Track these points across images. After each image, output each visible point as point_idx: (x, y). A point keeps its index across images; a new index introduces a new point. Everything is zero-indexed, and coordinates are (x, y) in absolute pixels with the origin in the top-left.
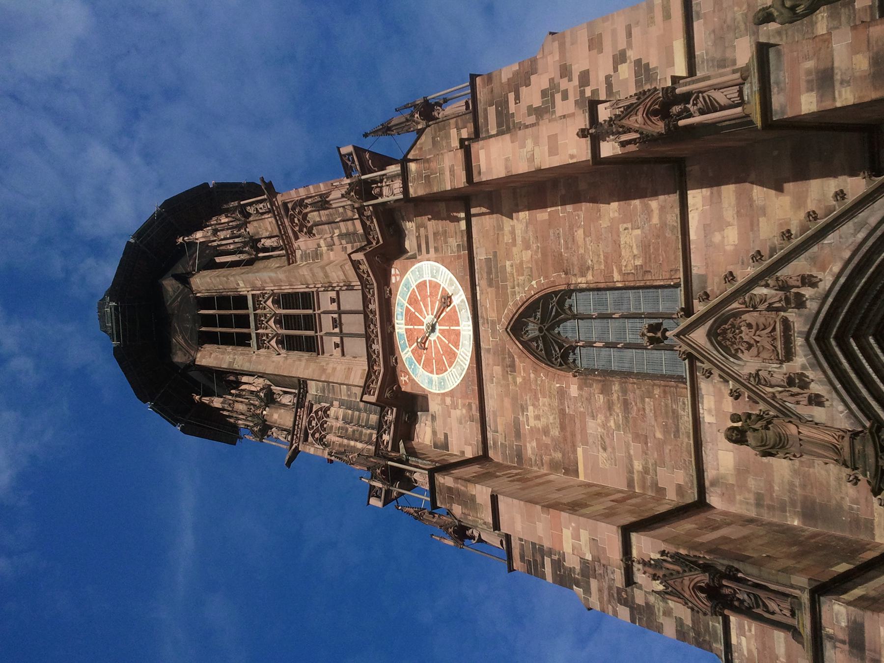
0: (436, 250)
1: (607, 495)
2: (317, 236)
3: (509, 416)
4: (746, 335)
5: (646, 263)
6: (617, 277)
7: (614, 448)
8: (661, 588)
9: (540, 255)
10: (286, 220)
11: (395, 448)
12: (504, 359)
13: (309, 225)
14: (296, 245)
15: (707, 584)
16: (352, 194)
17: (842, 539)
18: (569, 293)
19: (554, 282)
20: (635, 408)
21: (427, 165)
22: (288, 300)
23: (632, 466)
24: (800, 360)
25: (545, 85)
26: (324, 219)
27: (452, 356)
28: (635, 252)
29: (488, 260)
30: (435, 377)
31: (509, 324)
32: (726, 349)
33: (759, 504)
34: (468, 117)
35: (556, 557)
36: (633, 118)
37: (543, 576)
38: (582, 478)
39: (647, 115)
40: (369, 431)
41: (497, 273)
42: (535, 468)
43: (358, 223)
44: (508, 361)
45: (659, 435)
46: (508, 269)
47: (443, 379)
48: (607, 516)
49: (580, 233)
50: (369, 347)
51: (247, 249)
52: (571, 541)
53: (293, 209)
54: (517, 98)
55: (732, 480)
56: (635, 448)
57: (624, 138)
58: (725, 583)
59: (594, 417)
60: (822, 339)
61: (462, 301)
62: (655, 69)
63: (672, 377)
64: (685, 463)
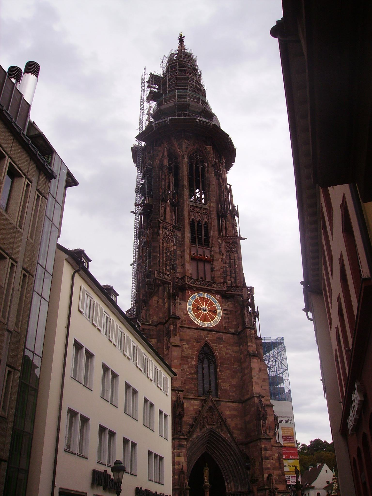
0: (225, 317)
6: (220, 381)
24: (208, 427)
29: (222, 339)
30: (191, 308)
44: (199, 340)
47: (191, 311)
49: (229, 372)
60: (211, 431)
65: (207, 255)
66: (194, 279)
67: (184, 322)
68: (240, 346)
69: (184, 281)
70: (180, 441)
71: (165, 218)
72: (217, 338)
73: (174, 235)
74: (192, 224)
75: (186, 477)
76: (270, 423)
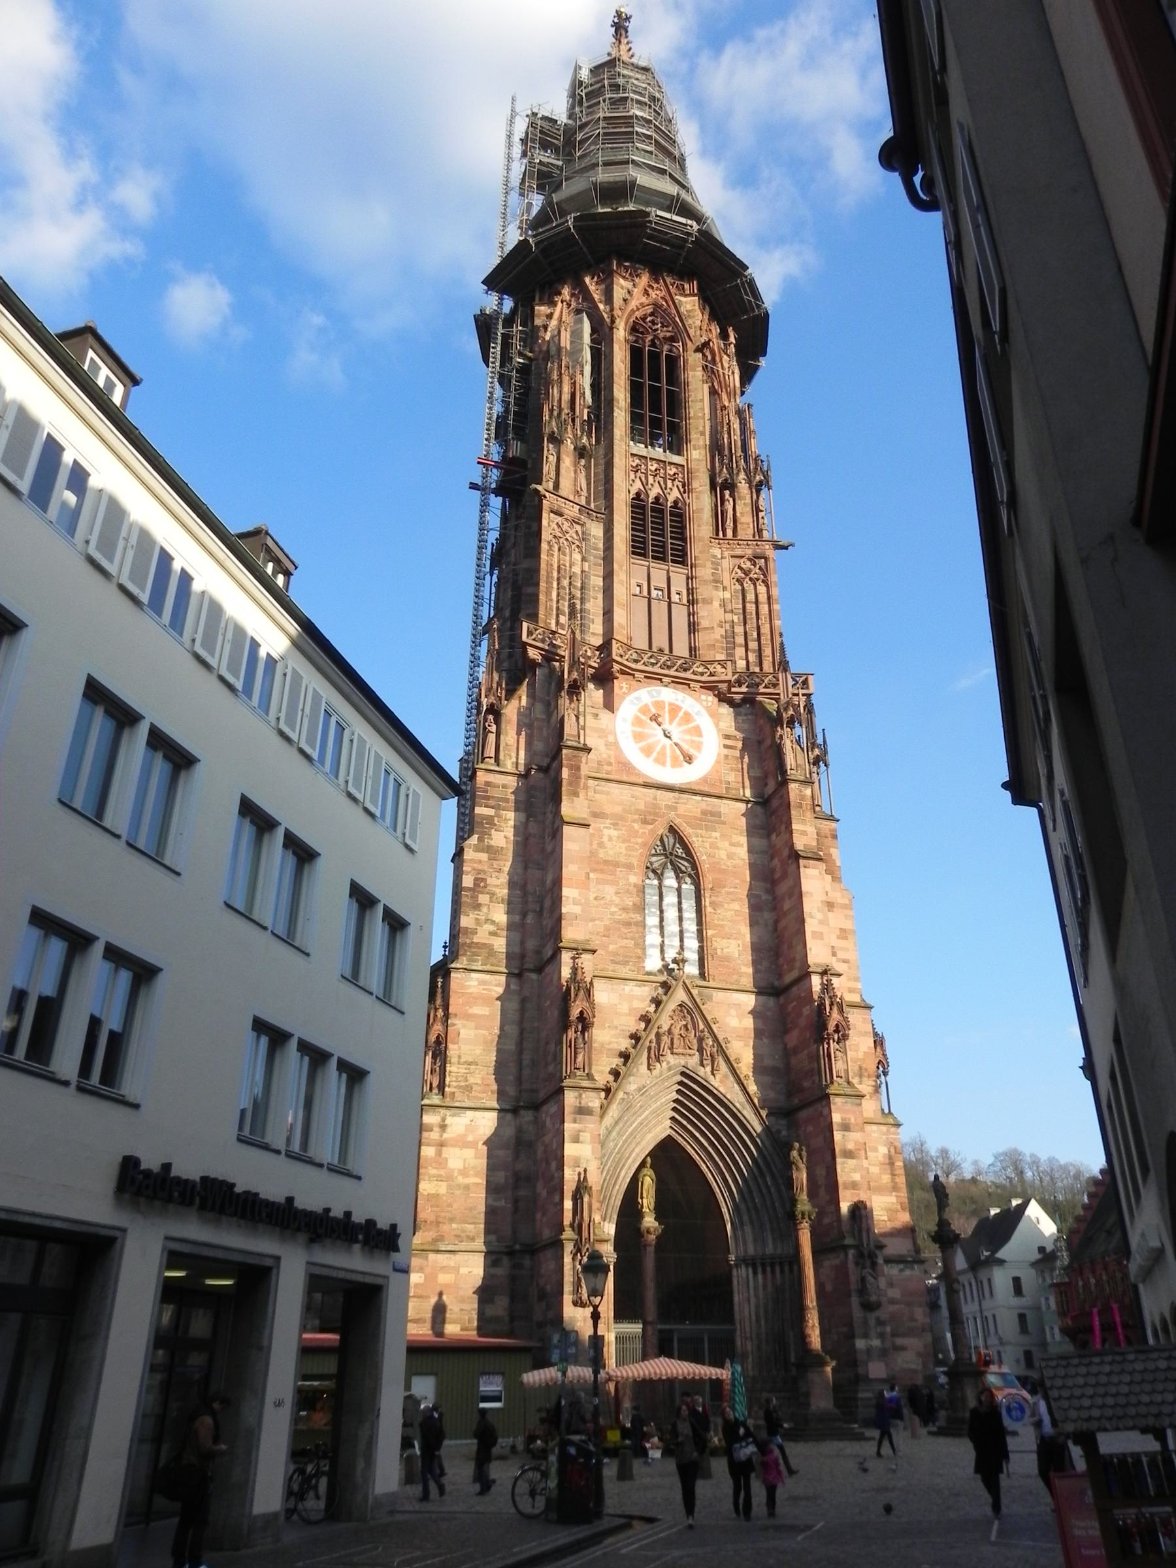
0: (726, 757)
3: (608, 809)
29: (719, 815)
44: (649, 818)
45: (611, 947)
46: (715, 834)
59: (617, 893)
66: (637, 651)
67: (605, 767)
68: (769, 836)
69: (610, 654)
70: (580, 1095)
71: (557, 486)
73: (583, 533)
74: (638, 504)
75: (595, 1205)
76: (861, 1055)
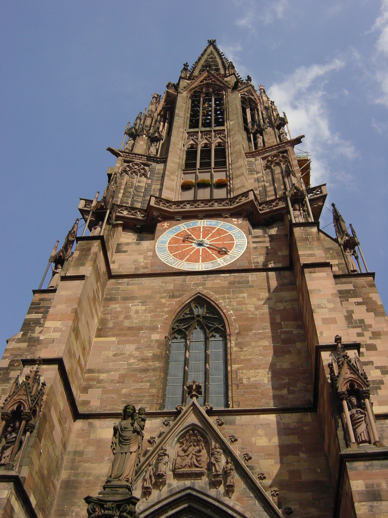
0: (255, 248)
1: (84, 354)
2: (264, 172)
4: (193, 450)
5: (244, 386)
6: (235, 367)
7: (115, 361)
8: (20, 381)
9: (250, 316)
10: (275, 152)
11: (118, 218)
12: (179, 291)
13: (272, 166)
14: (258, 158)
15: (22, 411)
16: (295, 191)
17: (52, 504)
18: (224, 336)
19: (232, 325)
20: (143, 376)
21: (315, 239)
22: (221, 152)
23: (103, 373)
24: (175, 484)
25: (367, 322)
26: (276, 176)
27: (181, 257)
28: (252, 379)
29: (248, 282)
30: (167, 245)
31: (203, 295)
32: (183, 436)
33: (75, 453)
34: (346, 271)
35: (42, 321)
36: (349, 371)
37: (29, 313)
38: (95, 340)
39: (351, 380)
40: (130, 202)
41: (239, 287)
42: (102, 309)
43: (274, 197)
44: (177, 294)
45: (124, 391)
46: (242, 295)
48: (70, 352)
50: (189, 202)
51: (255, 127)
52: (53, 326)
53: (283, 157)
54: (359, 304)
55: (92, 436)
56: (115, 375)
57: (335, 366)
58: (24, 422)
59: (137, 349)
61: (219, 264)
62: (377, 393)
63: (164, 401)
64: (105, 407)
65: (219, 176)
72: (230, 283)
